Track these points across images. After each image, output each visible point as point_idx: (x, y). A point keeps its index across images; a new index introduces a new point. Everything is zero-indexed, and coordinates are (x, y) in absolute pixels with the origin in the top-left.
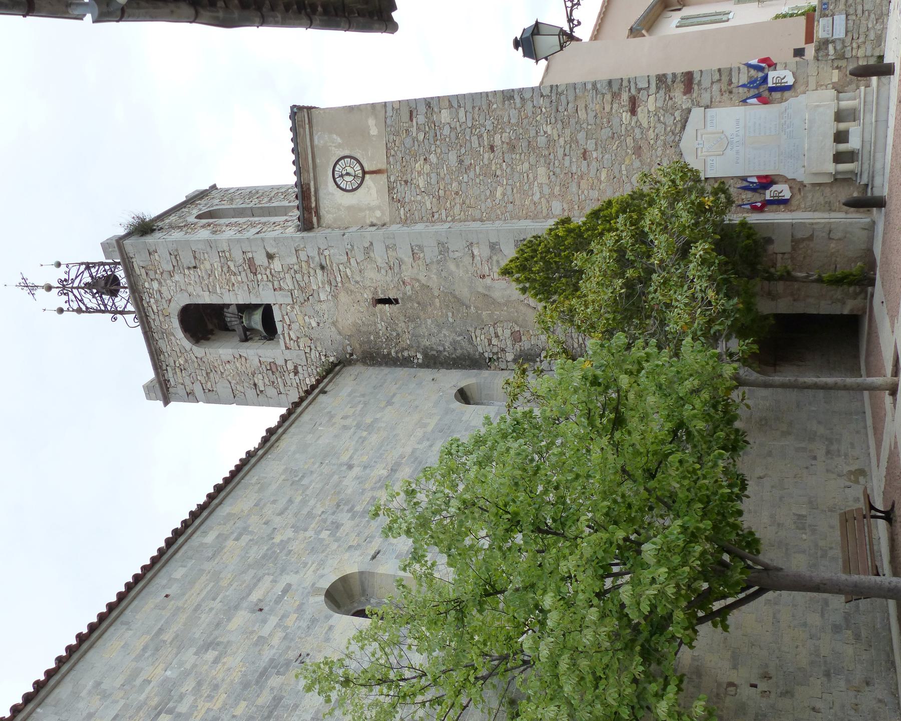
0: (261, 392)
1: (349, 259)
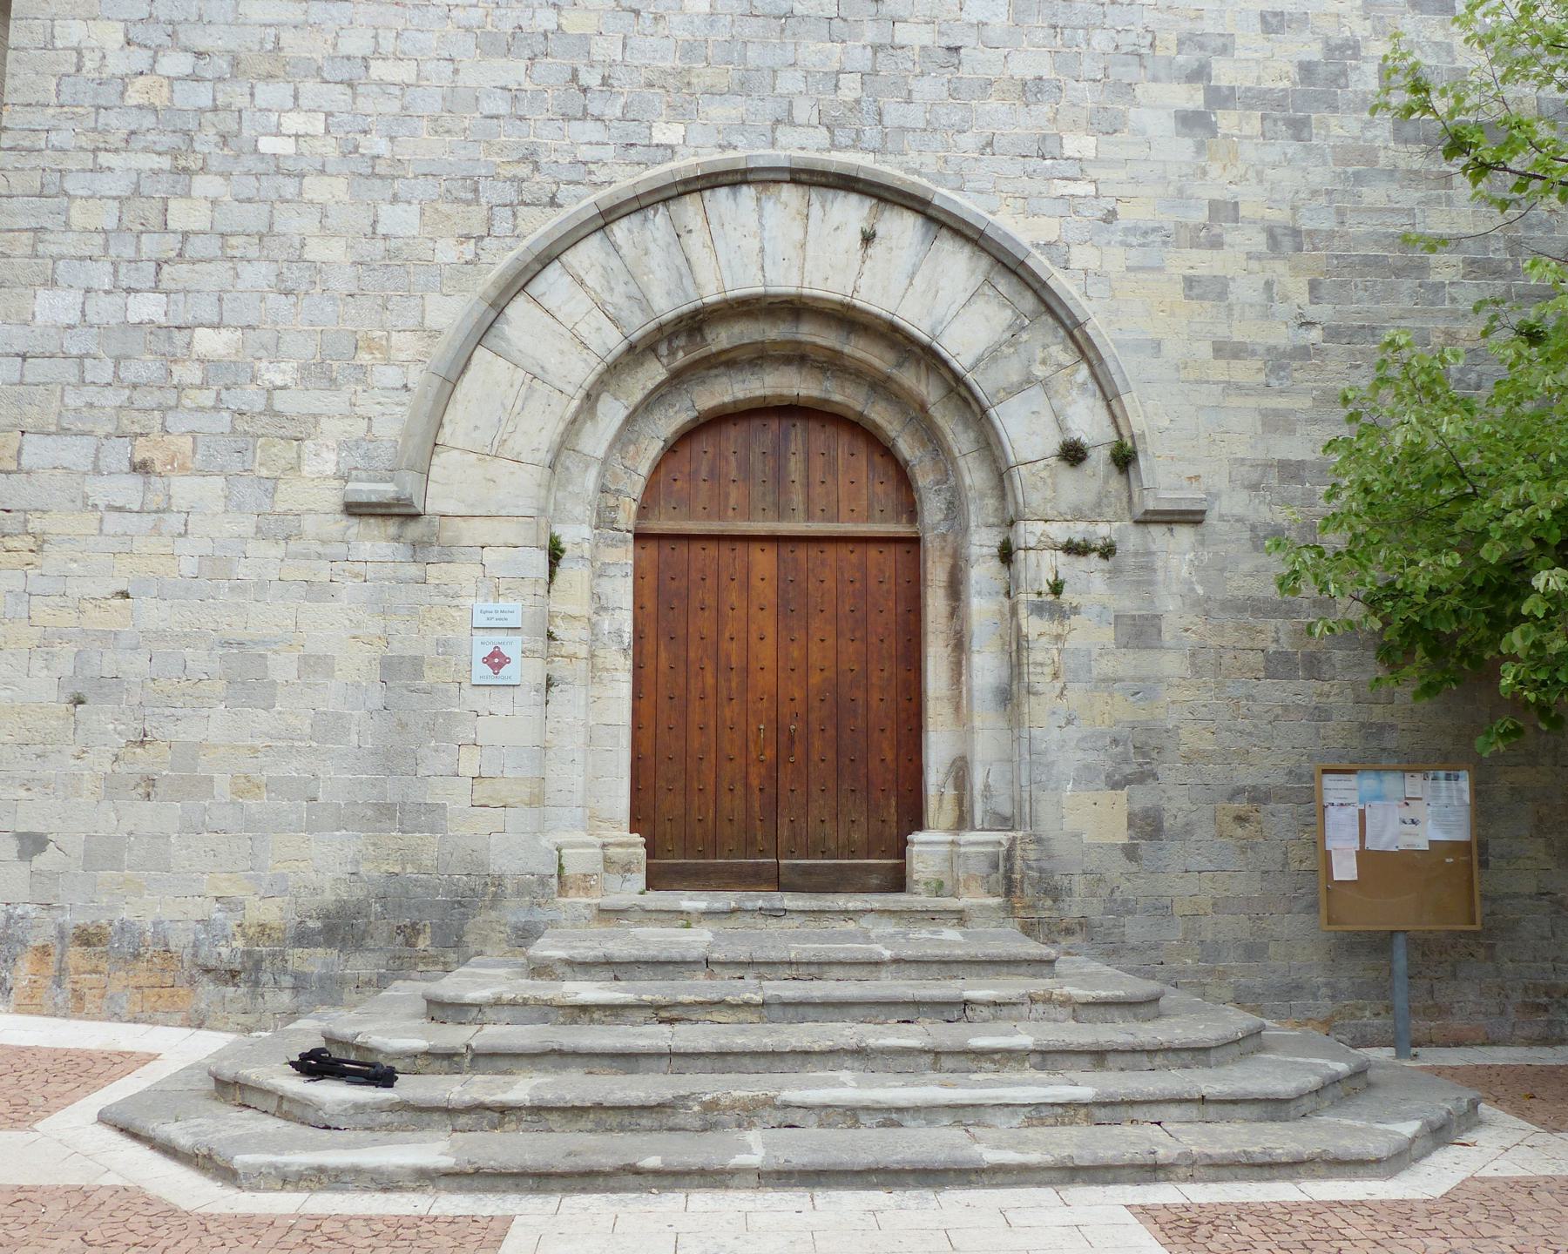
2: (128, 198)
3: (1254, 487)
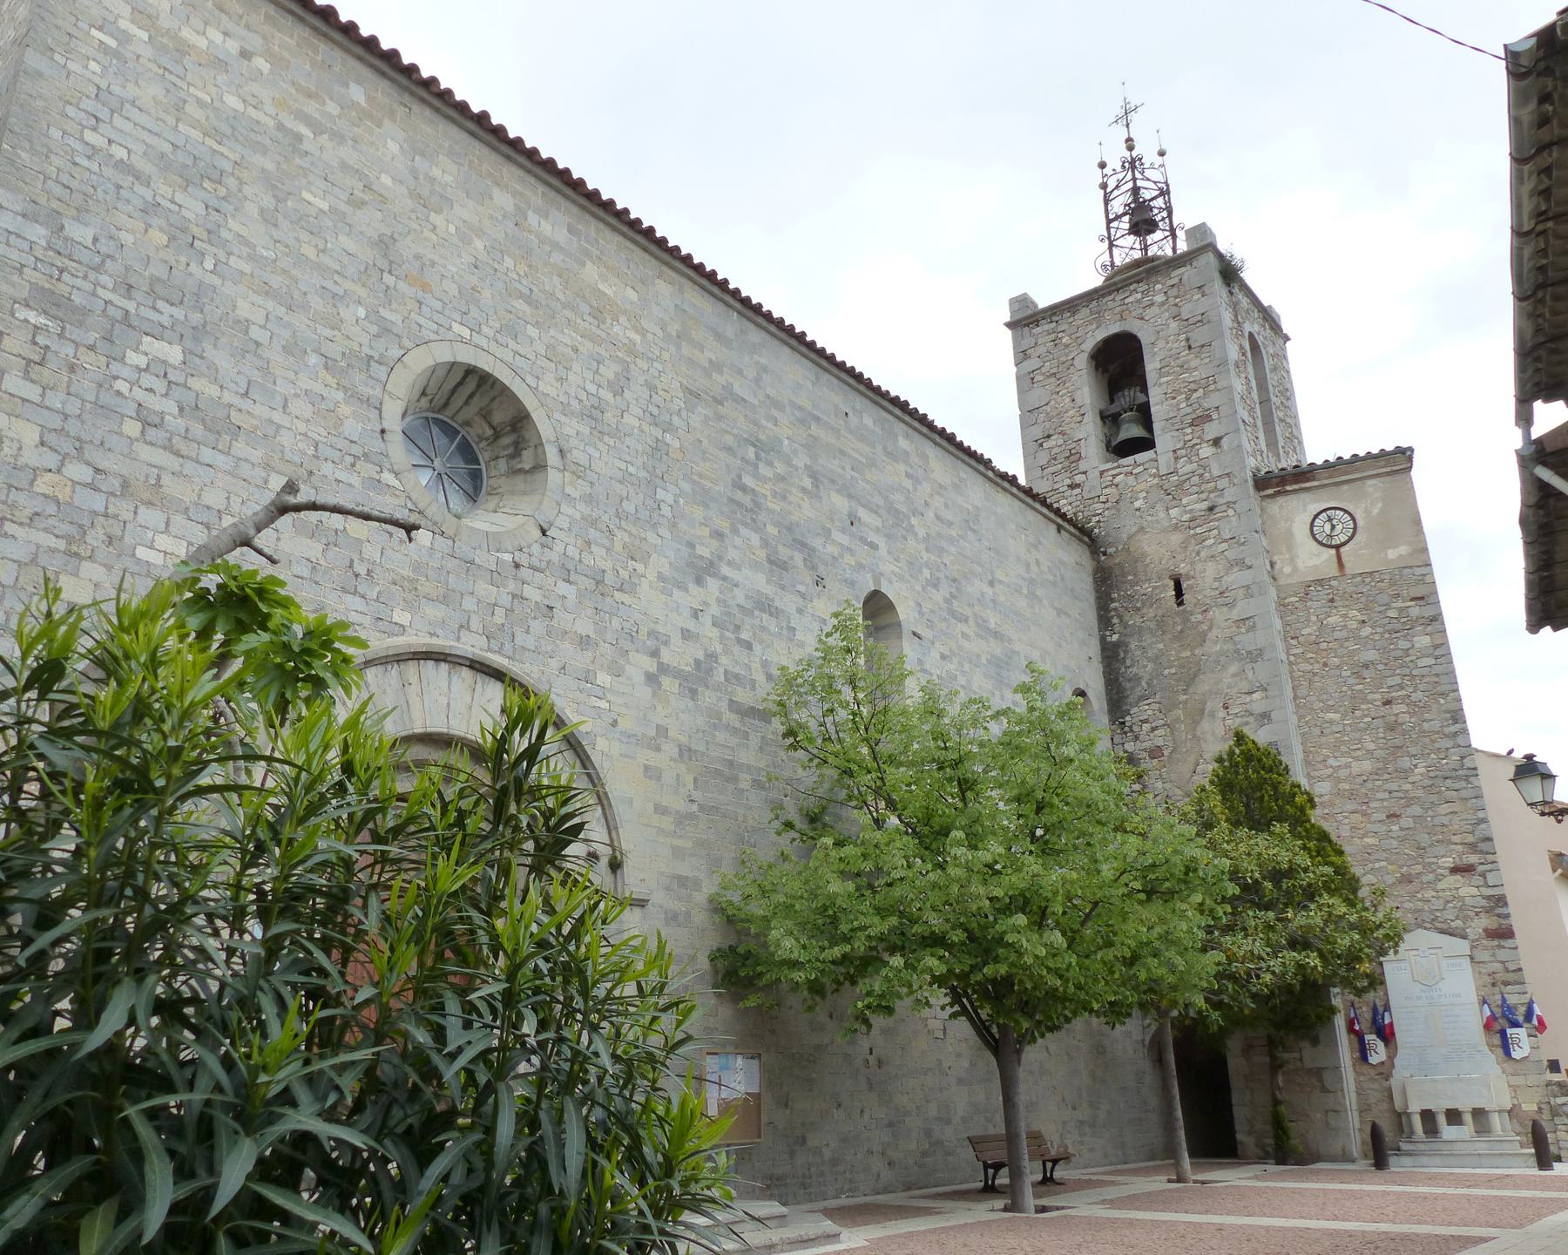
0: (1041, 445)
1: (1226, 541)
2: (26, 564)
3: (667, 889)
